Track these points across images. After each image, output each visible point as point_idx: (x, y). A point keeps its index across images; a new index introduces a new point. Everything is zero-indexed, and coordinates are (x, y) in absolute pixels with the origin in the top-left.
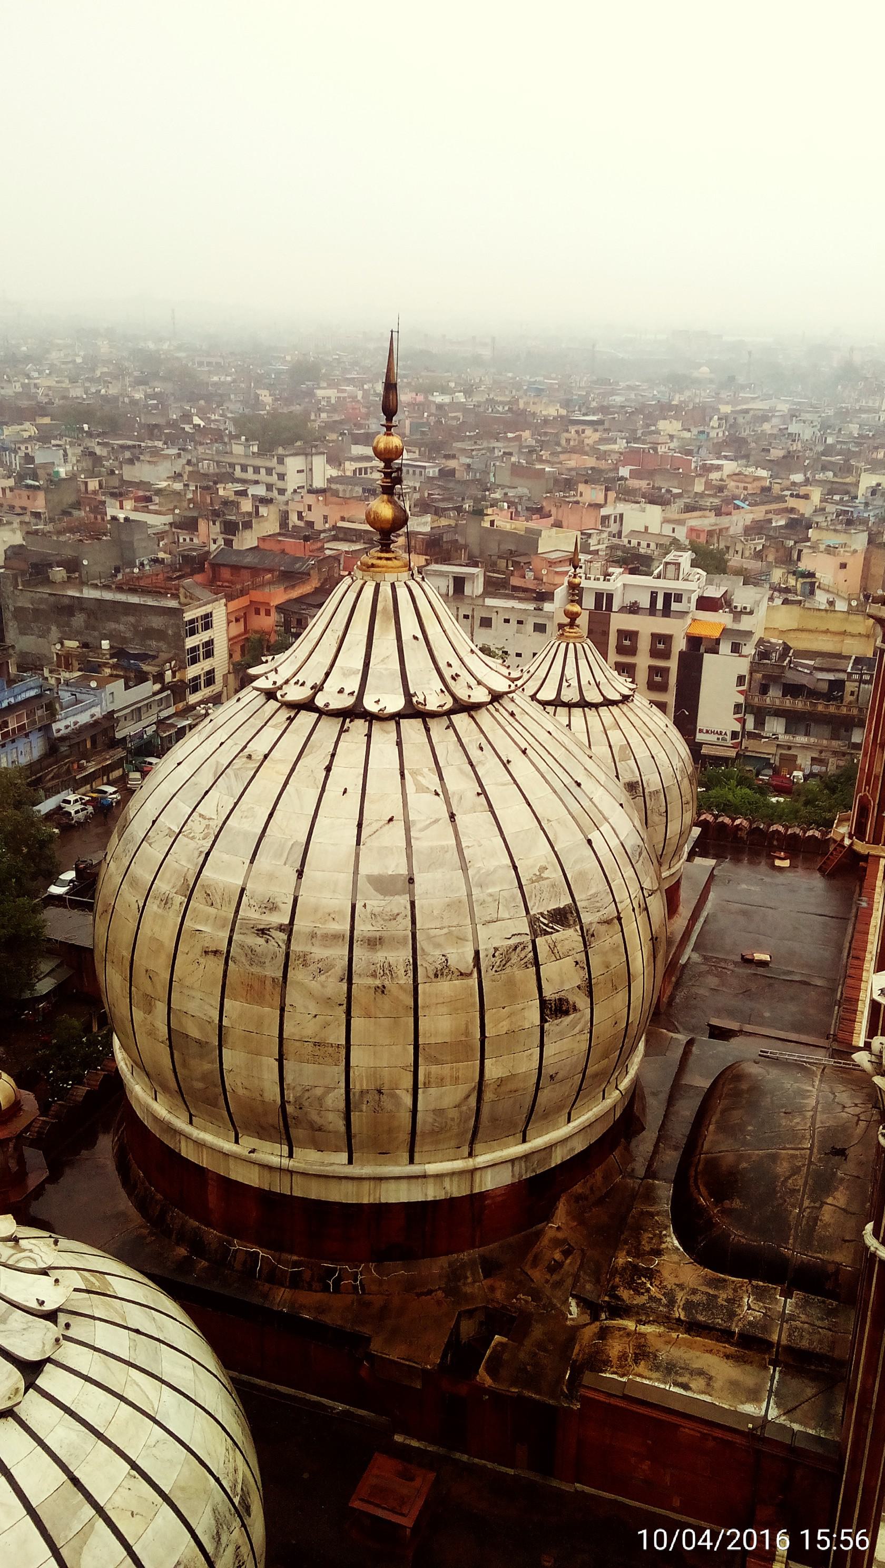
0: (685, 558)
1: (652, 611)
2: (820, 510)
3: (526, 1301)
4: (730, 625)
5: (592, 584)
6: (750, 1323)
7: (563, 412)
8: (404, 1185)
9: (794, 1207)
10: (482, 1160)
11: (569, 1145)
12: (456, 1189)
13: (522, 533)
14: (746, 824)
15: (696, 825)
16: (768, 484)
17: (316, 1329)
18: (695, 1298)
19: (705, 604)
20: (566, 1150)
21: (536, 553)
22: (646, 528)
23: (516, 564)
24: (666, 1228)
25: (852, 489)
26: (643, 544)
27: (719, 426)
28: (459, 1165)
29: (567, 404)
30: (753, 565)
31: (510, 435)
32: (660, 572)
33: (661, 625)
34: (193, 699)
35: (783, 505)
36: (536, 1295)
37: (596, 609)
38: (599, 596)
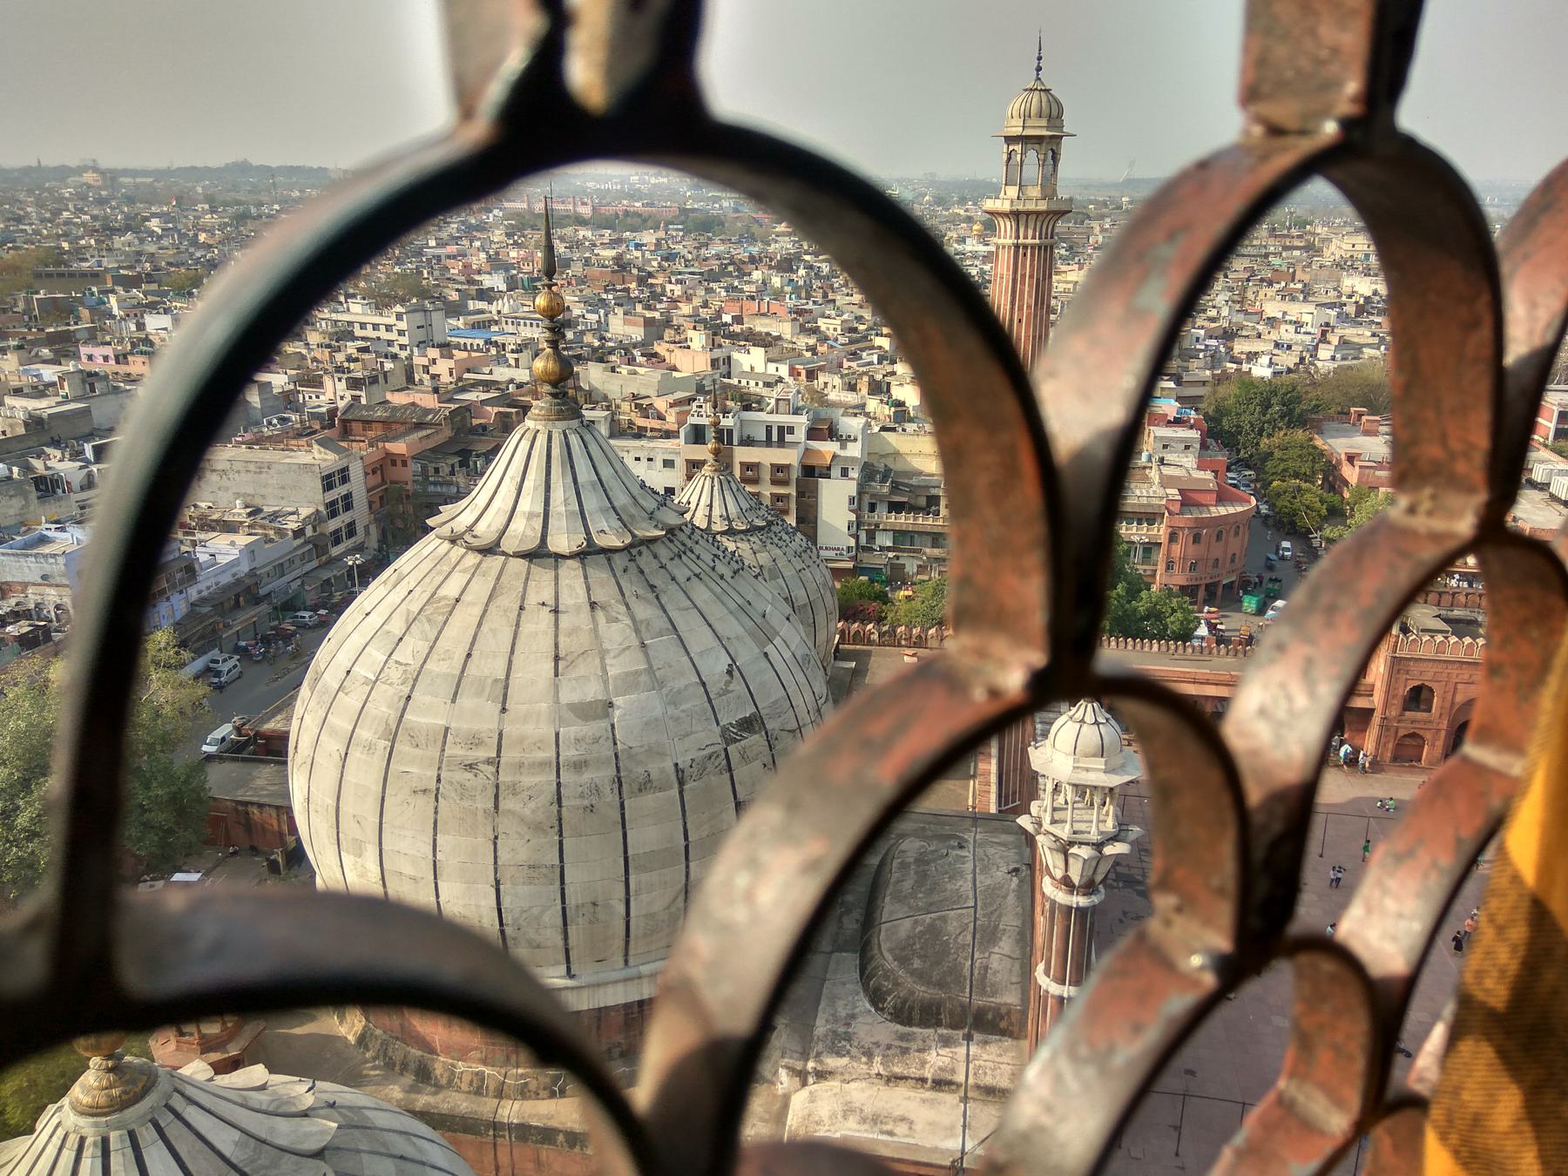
1: (768, 442)
6: (941, 1069)
8: (620, 988)
9: (966, 959)
22: (752, 368)
24: (857, 994)
26: (752, 383)
31: (619, 287)
35: (867, 344)
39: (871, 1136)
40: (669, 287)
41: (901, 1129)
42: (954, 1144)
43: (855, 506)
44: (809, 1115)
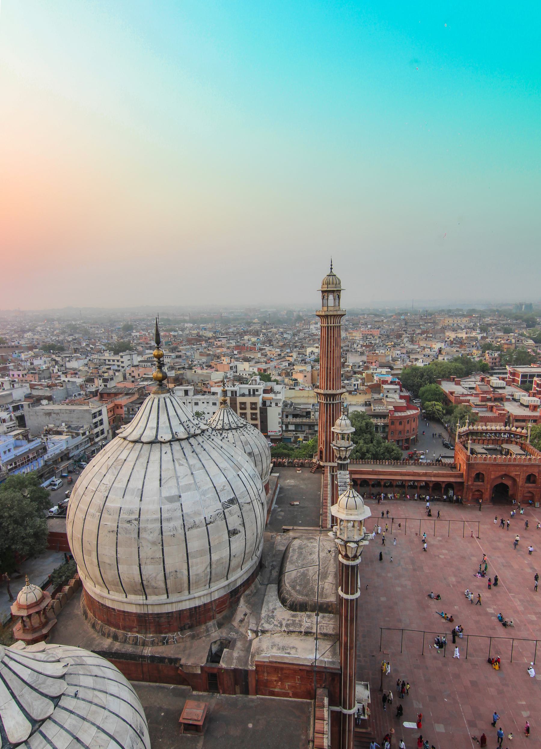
0: (258, 378)
3: (233, 634)
4: (274, 398)
5: (229, 388)
6: (307, 628)
7: (214, 335)
8: (187, 602)
10: (212, 589)
11: (242, 578)
12: (206, 600)
15: (271, 463)
17: (161, 659)
19: (265, 391)
20: (241, 580)
22: (245, 369)
23: (204, 384)
25: (304, 353)
26: (244, 374)
27: (263, 337)
28: (205, 592)
29: (215, 333)
30: (279, 378)
31: (198, 343)
33: (253, 399)
34: (97, 440)
35: (285, 359)
36: (237, 632)
37: (232, 396)
38: (232, 392)
39: (281, 655)
40: (216, 343)
41: (293, 651)
42: (312, 657)
43: (281, 416)
44: (259, 648)
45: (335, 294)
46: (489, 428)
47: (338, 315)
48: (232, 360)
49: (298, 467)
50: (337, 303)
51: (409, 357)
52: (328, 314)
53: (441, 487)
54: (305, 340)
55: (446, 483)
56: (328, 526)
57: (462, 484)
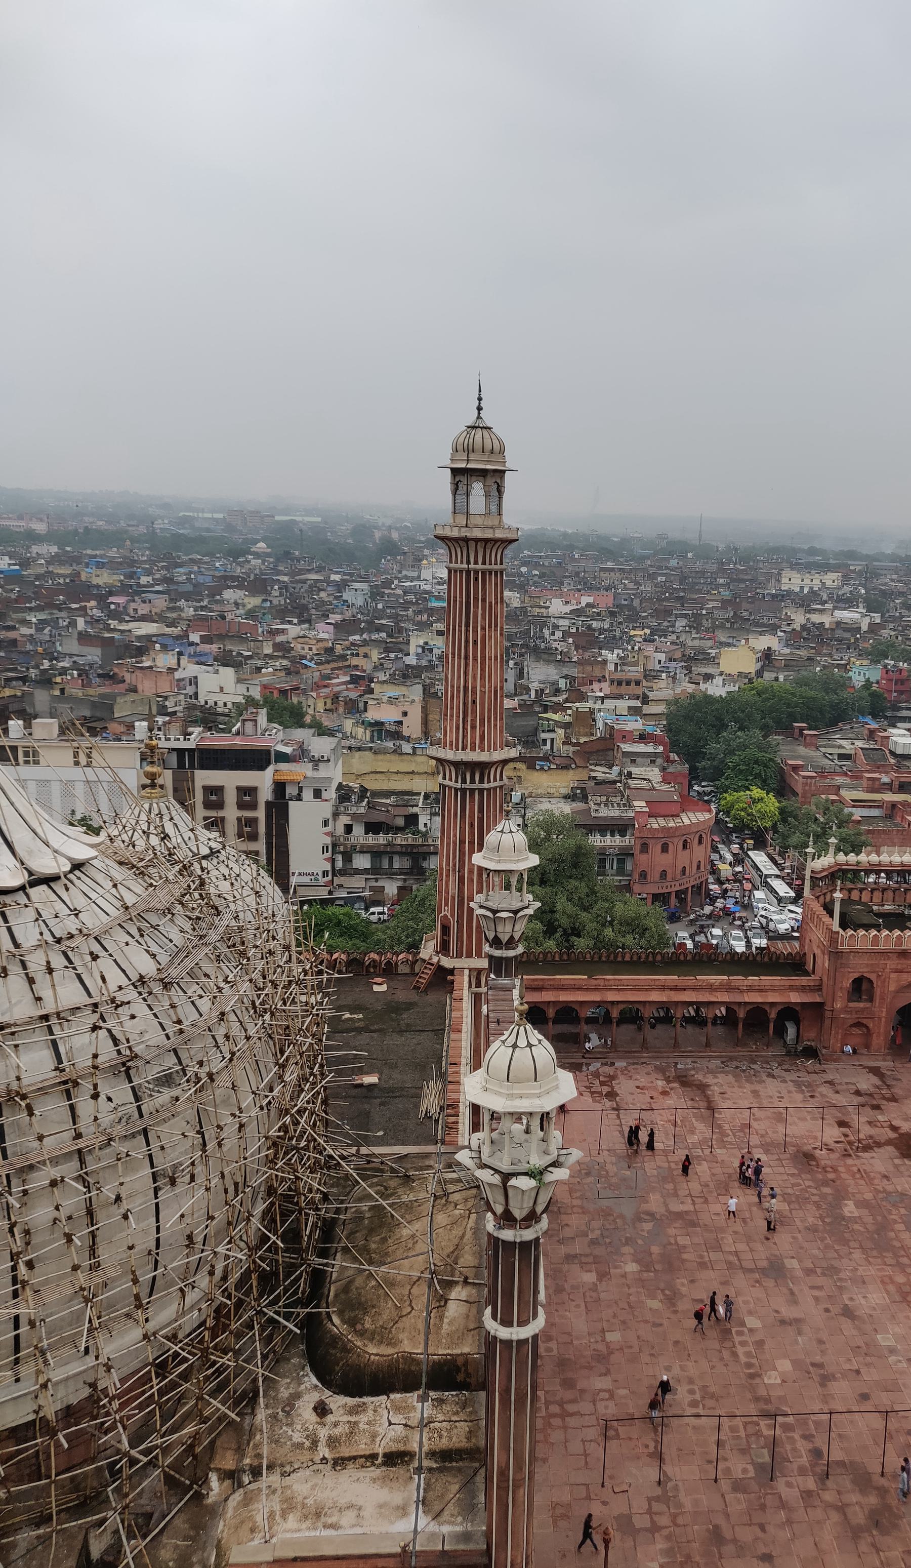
2: (379, 667)
4: (310, 773)
13: (96, 699)
14: (344, 957)
16: (331, 645)
18: (337, 1431)
21: (113, 719)
22: (222, 689)
25: (403, 647)
27: (281, 595)
31: (74, 606)
32: (239, 729)
35: (345, 663)
41: (347, 1518)
42: (404, 1526)
45: (490, 481)
46: (885, 858)
47: (495, 541)
48: (184, 660)
49: (379, 976)
50: (494, 508)
51: (689, 669)
52: (469, 535)
53: (768, 1021)
54: (407, 609)
55: (780, 1008)
56: (460, 1139)
57: (818, 1007)
